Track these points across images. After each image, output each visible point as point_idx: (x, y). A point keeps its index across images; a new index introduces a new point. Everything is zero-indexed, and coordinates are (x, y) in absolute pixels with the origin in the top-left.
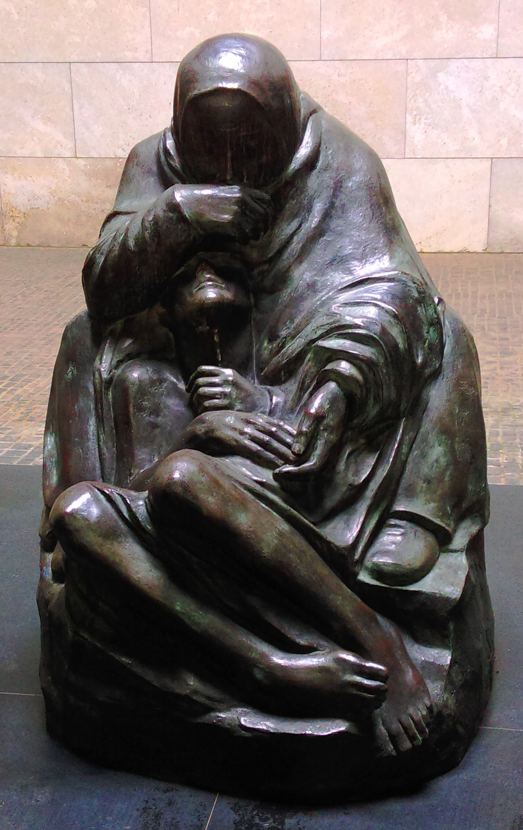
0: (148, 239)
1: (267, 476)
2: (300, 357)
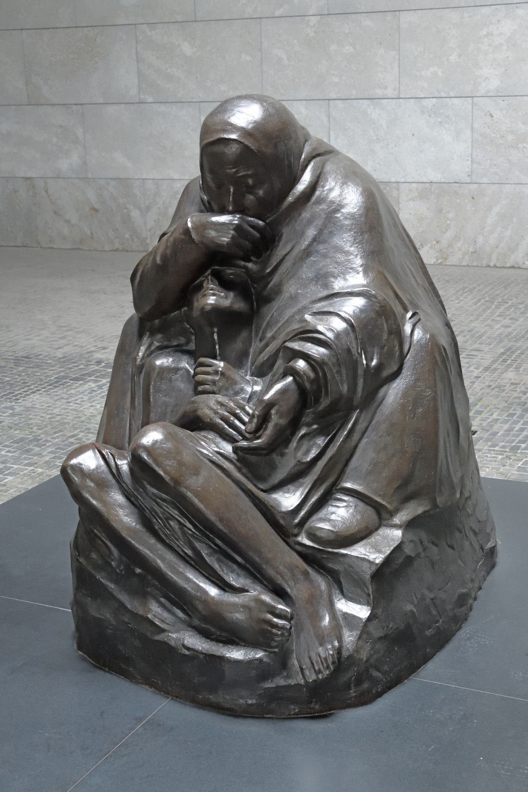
0: (169, 256)
1: (227, 448)
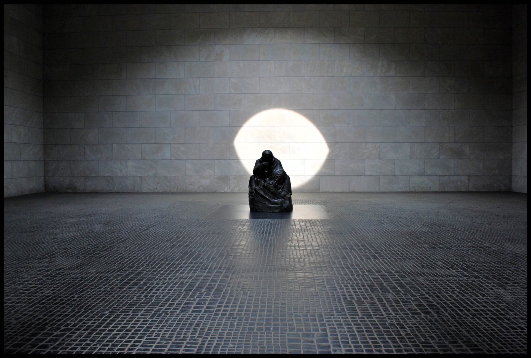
2: (274, 177)
